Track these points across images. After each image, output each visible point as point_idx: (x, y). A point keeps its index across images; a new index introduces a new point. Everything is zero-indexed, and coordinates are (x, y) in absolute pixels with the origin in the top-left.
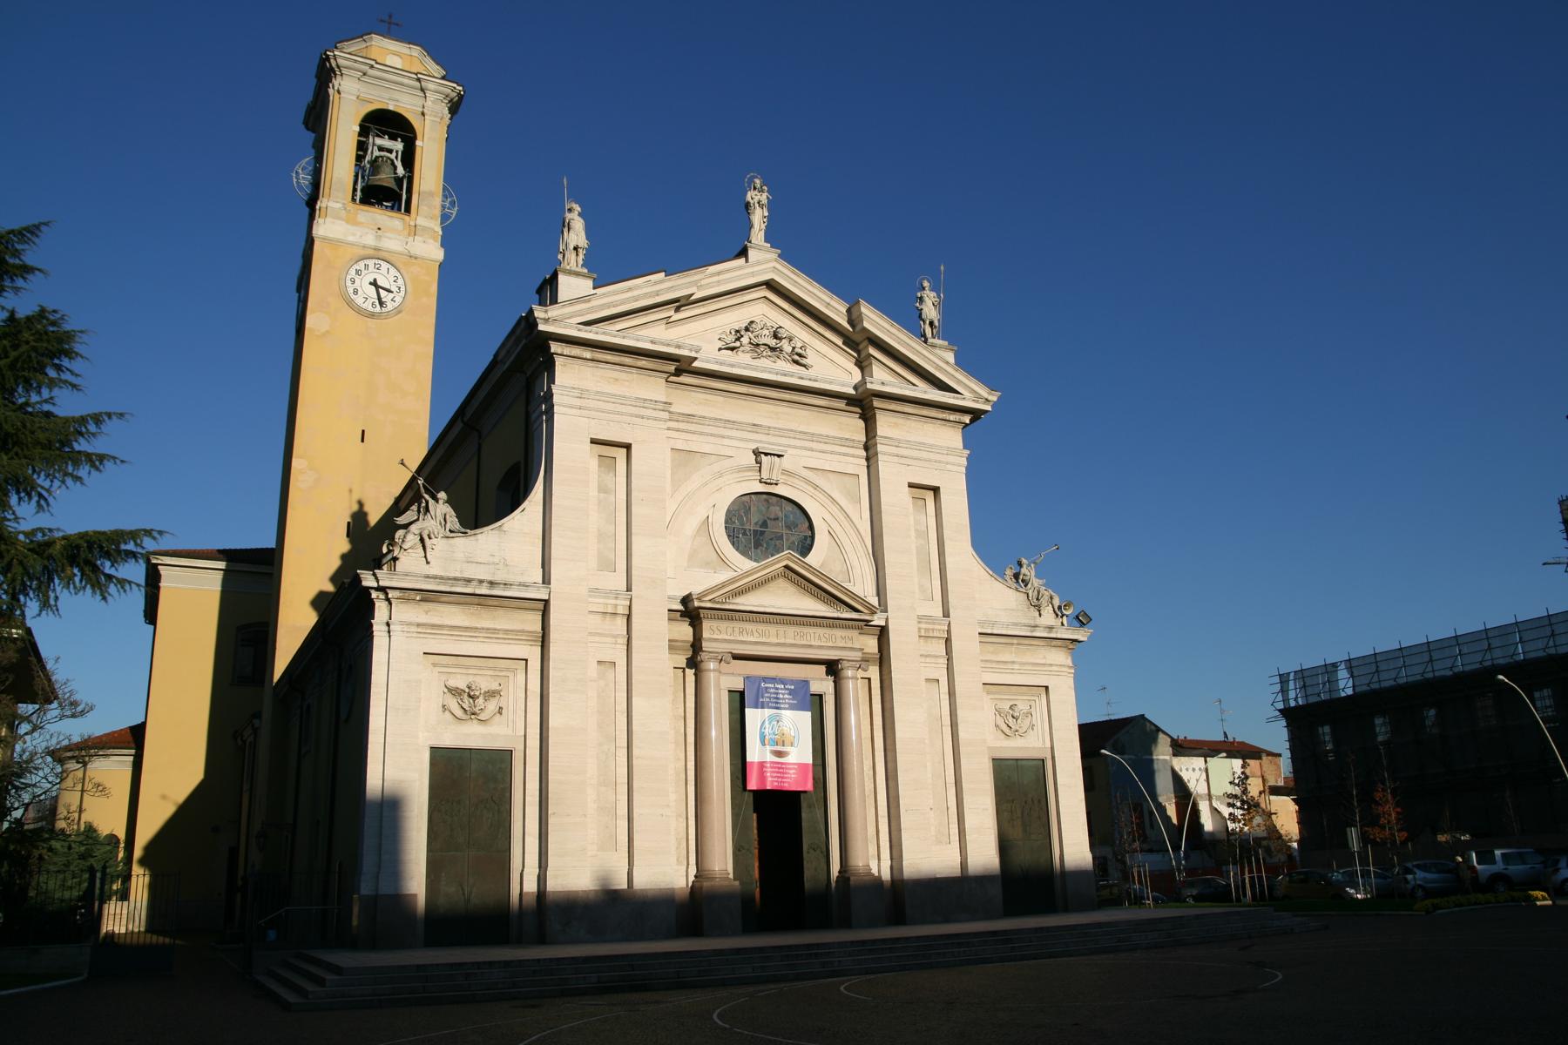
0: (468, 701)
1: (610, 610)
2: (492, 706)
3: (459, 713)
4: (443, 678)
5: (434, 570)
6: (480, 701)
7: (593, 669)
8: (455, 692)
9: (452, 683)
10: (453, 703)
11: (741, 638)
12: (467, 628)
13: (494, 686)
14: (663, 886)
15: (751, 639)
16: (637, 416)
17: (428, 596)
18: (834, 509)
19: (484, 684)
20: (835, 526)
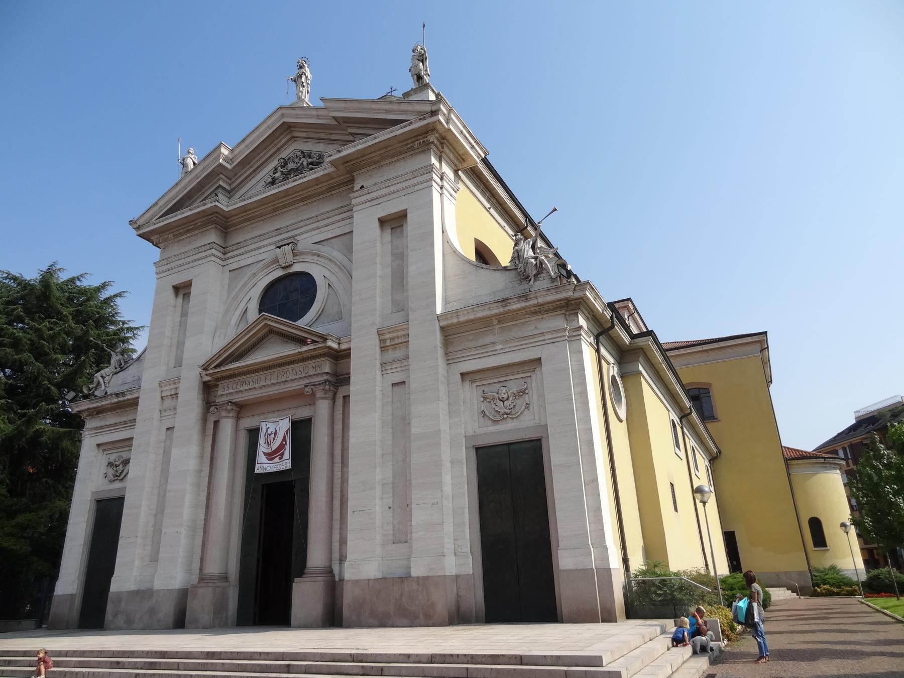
16: (196, 260)
18: (331, 266)
20: (333, 279)
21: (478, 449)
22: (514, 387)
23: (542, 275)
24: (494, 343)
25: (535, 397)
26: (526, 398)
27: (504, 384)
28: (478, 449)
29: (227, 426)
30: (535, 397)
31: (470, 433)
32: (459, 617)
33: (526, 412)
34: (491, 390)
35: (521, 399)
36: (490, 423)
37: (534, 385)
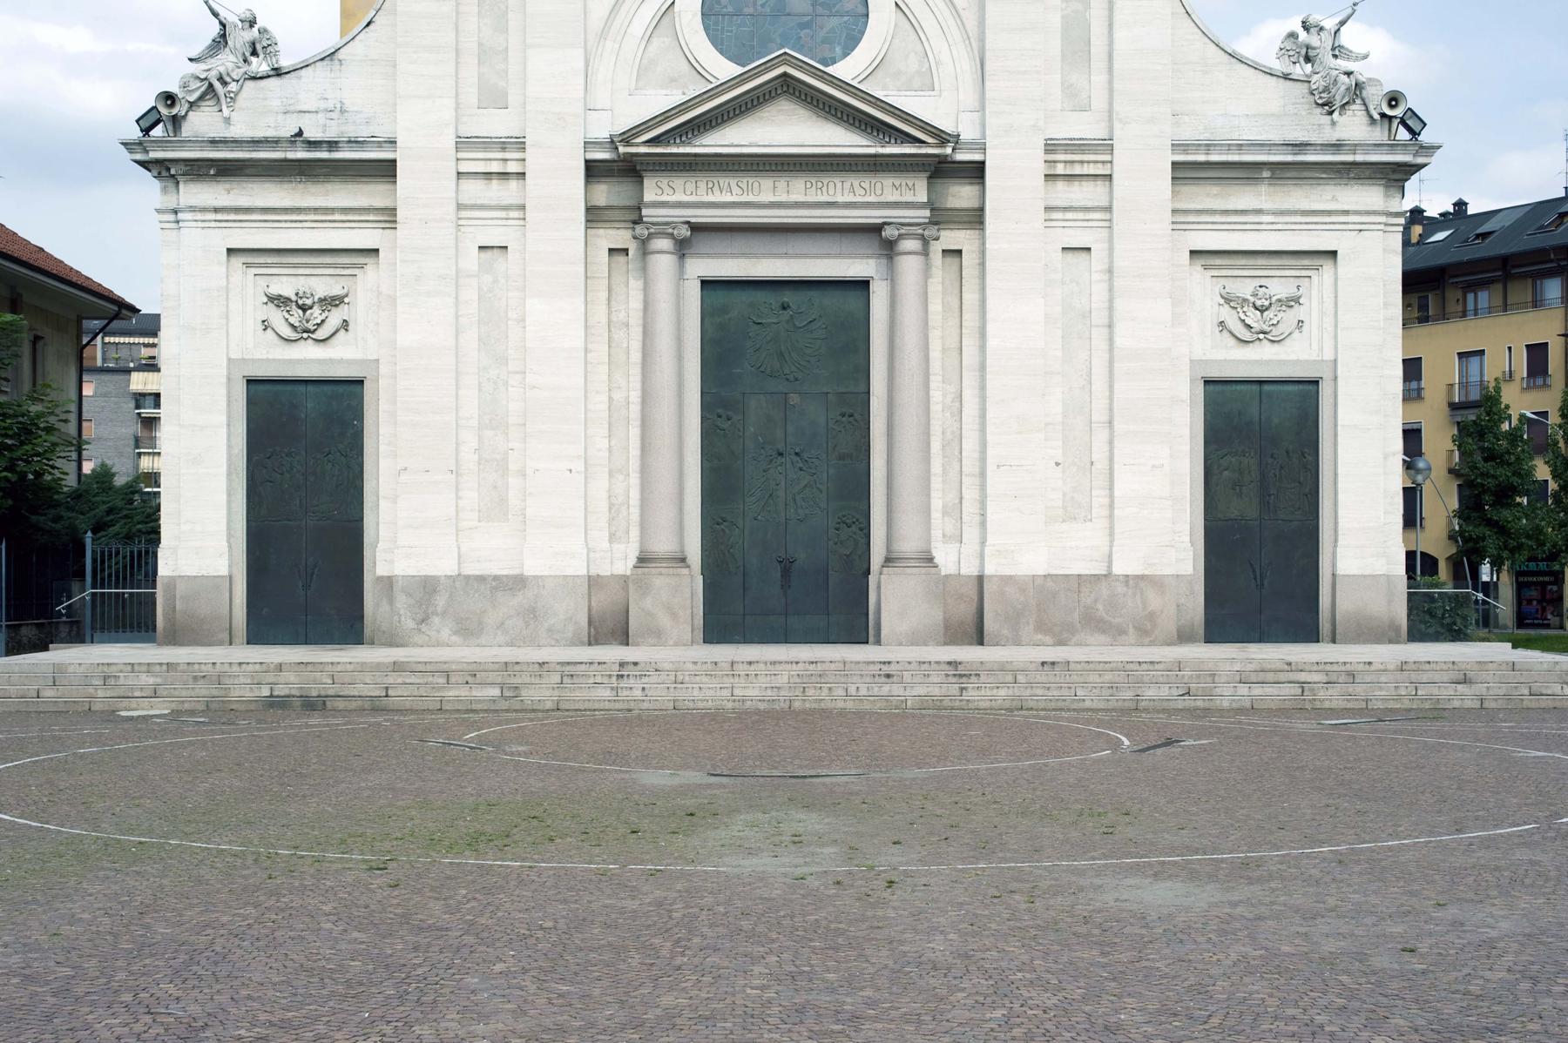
0: (304, 317)
1: (495, 167)
2: (335, 318)
3: (287, 332)
4: (262, 282)
5: (239, 130)
6: (316, 314)
7: (472, 258)
8: (279, 301)
9: (275, 289)
10: (276, 317)
11: (711, 198)
12: (286, 210)
13: (337, 291)
14: (329, 186)
15: (728, 198)
17: (227, 170)
19: (322, 286)
21: (1207, 382)
22: (1279, 288)
23: (1353, 107)
24: (1259, 212)
25: (1315, 314)
26: (1297, 313)
27: (1263, 282)
28: (1207, 382)
29: (663, 263)
30: (1315, 314)
31: (1198, 355)
32: (1184, 637)
33: (1296, 334)
34: (1245, 289)
35: (1291, 312)
36: (1232, 341)
37: (1315, 293)
